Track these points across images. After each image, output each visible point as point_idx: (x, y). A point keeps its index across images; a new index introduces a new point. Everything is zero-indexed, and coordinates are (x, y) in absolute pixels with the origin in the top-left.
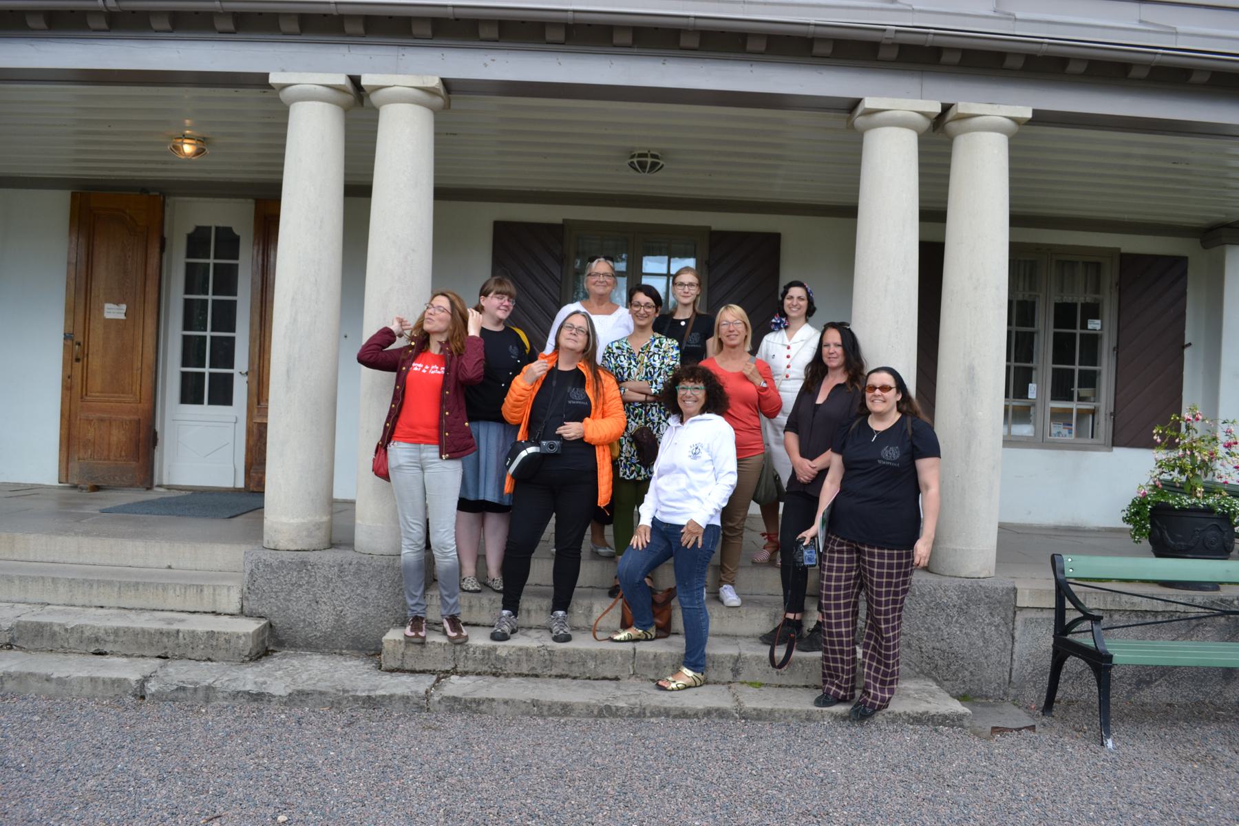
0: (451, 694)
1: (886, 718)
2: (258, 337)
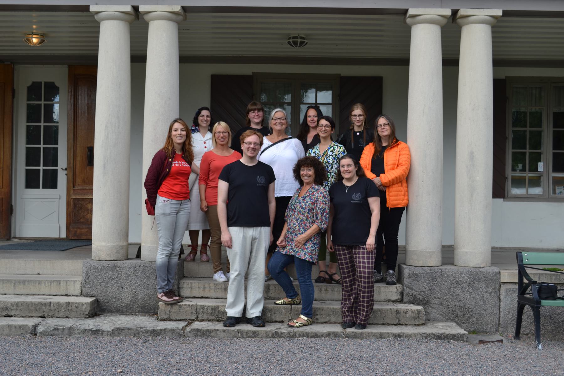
0: (197, 328)
1: (422, 336)
2: (72, 147)
